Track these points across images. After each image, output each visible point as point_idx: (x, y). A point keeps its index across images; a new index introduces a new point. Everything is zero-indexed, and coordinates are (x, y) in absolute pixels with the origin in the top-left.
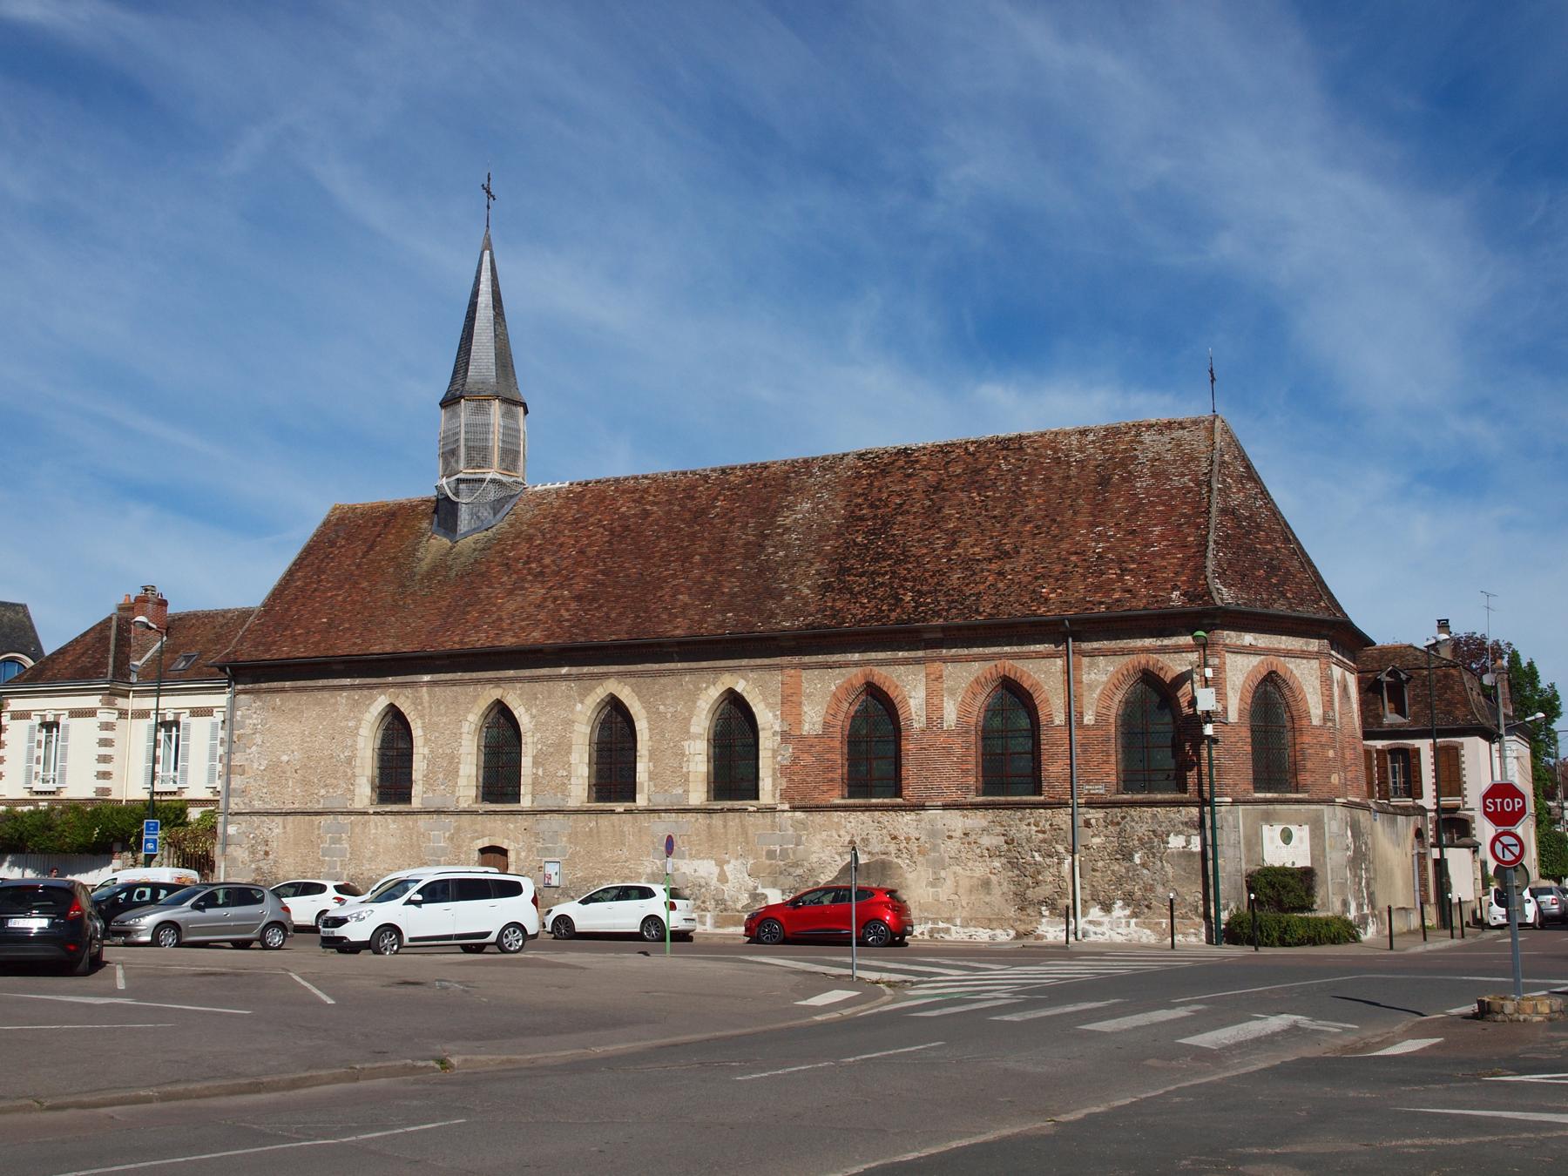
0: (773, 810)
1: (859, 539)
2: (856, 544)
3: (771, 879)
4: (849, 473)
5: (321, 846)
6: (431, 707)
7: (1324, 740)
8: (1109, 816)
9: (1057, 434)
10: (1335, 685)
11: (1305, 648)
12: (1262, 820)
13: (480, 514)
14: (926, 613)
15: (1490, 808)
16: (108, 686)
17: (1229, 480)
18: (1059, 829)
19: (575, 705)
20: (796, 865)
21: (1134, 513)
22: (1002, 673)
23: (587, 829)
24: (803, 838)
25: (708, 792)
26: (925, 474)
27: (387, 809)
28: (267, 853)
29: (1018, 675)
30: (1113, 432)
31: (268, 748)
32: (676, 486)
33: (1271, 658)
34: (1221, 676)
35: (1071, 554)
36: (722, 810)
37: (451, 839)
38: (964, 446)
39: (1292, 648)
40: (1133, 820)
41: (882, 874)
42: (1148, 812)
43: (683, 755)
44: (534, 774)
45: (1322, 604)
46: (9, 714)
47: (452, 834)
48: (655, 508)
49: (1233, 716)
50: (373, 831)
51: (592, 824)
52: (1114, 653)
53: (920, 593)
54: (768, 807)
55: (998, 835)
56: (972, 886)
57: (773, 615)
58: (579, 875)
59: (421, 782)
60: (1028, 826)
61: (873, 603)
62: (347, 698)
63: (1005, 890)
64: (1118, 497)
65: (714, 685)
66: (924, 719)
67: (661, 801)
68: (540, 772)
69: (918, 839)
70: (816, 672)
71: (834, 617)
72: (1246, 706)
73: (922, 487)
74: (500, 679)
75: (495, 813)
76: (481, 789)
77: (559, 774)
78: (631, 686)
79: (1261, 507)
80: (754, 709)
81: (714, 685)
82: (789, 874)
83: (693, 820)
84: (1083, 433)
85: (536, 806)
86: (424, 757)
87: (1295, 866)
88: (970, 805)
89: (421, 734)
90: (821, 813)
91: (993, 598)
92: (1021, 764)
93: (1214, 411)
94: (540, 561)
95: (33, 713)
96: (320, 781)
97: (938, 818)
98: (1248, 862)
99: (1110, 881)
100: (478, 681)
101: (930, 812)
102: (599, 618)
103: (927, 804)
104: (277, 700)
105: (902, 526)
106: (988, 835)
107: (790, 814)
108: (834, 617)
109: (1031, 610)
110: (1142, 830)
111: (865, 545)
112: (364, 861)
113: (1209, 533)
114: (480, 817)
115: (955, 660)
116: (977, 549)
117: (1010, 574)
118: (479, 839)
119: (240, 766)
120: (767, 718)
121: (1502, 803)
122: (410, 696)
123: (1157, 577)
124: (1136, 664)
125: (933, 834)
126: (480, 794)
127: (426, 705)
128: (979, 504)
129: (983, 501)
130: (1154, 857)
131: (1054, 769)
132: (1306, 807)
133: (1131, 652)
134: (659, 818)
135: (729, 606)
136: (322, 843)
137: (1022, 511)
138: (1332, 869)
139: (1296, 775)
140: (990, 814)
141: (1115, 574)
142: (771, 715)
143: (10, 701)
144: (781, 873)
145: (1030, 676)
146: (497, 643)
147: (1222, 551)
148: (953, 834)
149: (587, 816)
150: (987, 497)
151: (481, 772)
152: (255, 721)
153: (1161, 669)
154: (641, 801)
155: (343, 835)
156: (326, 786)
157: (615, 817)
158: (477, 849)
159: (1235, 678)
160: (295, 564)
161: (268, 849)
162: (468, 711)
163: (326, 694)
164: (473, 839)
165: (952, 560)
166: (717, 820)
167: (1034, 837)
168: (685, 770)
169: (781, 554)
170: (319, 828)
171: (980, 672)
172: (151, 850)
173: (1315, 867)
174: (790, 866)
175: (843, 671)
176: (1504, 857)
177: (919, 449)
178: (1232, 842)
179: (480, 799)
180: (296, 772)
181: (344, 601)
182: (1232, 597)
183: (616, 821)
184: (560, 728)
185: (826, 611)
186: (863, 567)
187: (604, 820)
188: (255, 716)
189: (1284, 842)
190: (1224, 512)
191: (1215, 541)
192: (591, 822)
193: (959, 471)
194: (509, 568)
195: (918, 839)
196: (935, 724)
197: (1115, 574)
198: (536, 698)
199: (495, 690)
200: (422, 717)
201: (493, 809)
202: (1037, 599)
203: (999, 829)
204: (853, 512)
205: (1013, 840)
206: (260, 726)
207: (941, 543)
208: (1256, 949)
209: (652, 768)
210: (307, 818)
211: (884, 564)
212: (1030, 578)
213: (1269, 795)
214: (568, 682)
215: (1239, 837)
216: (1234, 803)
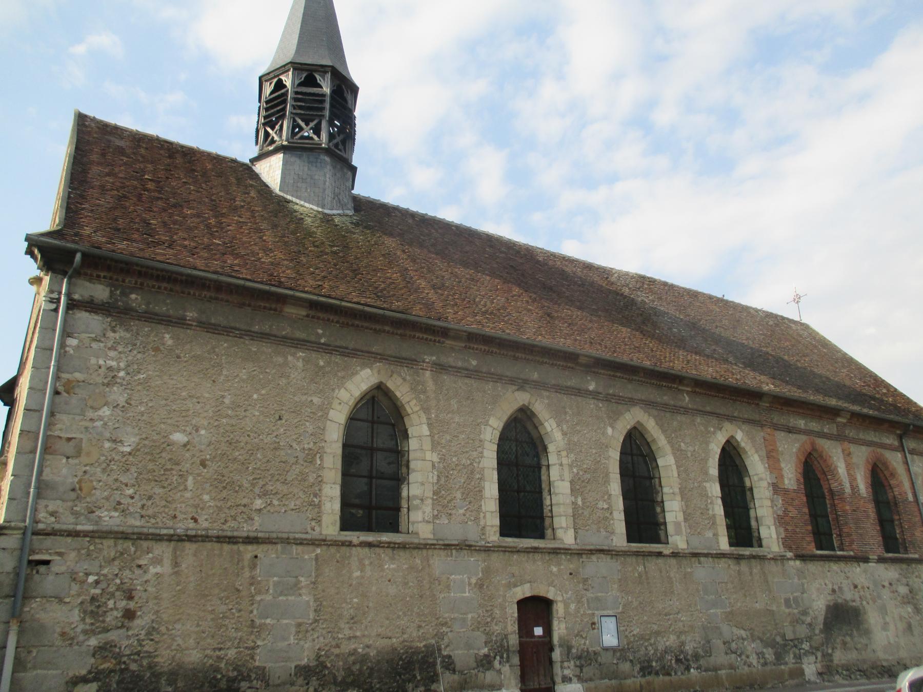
23: (637, 575)
28: (129, 615)
31: (142, 414)
37: (480, 586)
44: (573, 503)
47: (480, 579)
50: (358, 574)
51: (641, 568)
58: (635, 632)
59: (430, 501)
62: (306, 361)
68: (580, 502)
78: (655, 417)
82: (803, 623)
86: (433, 466)
89: (428, 433)
96: (253, 485)
100: (499, 378)
112: (342, 625)
118: (515, 586)
119: (69, 439)
122: (408, 378)
136: (259, 592)
152: (114, 364)
155: (302, 579)
157: (660, 561)
158: (516, 601)
161: (132, 605)
163: (267, 348)
164: (512, 585)
166: (744, 566)
168: (710, 512)
170: (253, 566)
184: (594, 451)
188: (112, 354)
195: (868, 588)
198: (566, 413)
199: (516, 393)
200: (426, 410)
203: (904, 581)
206: (122, 374)
209: (684, 507)
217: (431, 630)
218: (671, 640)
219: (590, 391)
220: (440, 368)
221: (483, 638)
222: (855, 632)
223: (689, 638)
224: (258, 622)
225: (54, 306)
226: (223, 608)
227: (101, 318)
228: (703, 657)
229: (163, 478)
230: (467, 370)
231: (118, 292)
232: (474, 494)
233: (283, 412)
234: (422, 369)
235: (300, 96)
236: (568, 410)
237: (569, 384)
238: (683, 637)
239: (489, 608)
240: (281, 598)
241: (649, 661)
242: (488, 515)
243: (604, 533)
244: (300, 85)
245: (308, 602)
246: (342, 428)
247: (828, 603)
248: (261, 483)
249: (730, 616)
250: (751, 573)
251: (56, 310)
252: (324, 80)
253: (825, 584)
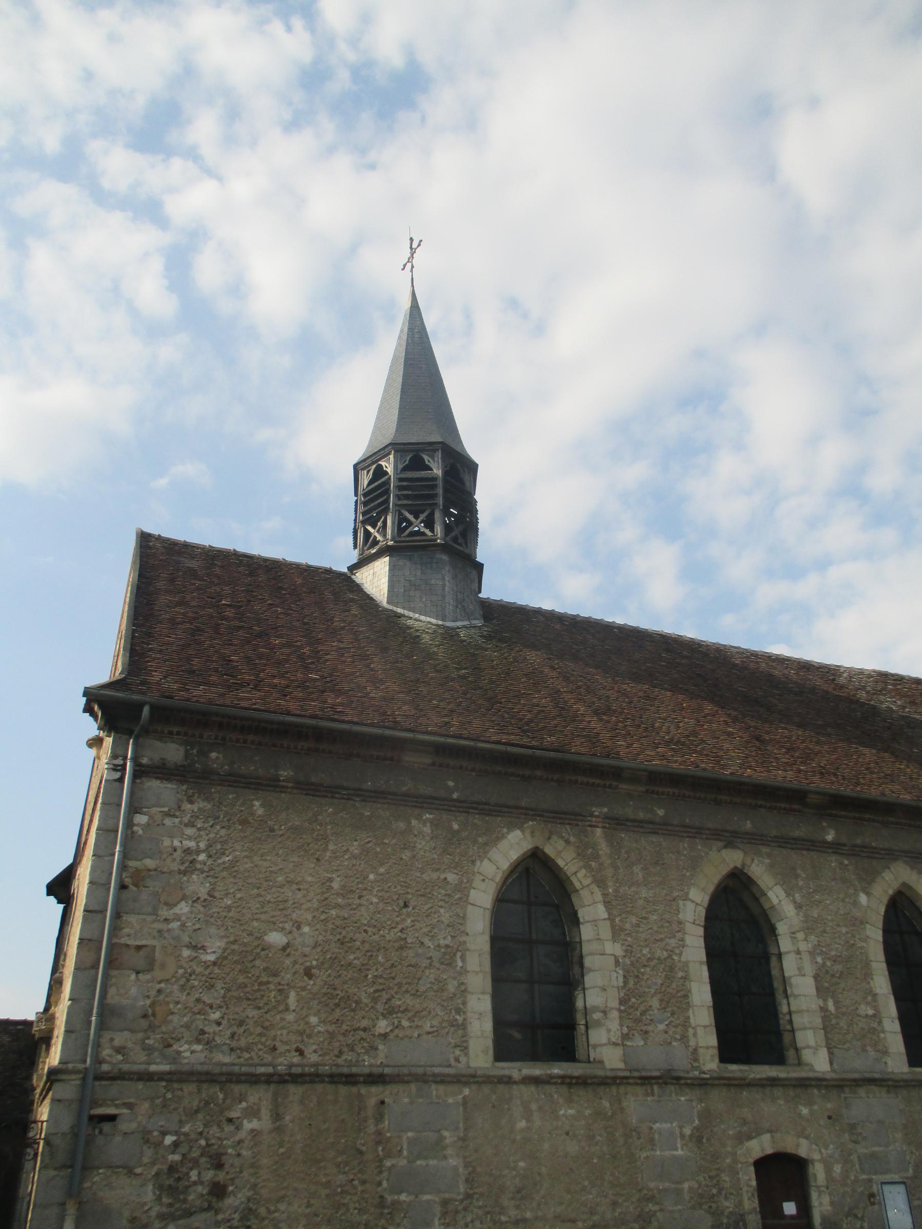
5: (388, 1163)
6: (616, 868)
28: (218, 1191)
31: (229, 908)
37: (697, 1138)
44: (821, 1008)
47: (697, 1129)
50: (522, 1124)
59: (615, 1014)
86: (617, 963)
89: (606, 916)
96: (375, 1000)
100: (696, 832)
112: (506, 1203)
118: (750, 1138)
119: (139, 948)
122: (572, 839)
136: (389, 1155)
152: (192, 844)
155: (446, 1133)
158: (752, 1161)
161: (221, 1176)
164: (742, 1138)
170: (379, 1117)
180: (308, 973)
184: (844, 930)
188: (189, 831)
199: (724, 852)
200: (600, 883)
206: (202, 857)
217: (631, 1209)
219: (829, 843)
220: (616, 823)
224: (389, 1198)
225: (117, 775)
226: (342, 1178)
227: (174, 786)
229: (258, 994)
230: (652, 823)
231: (195, 751)
233: (410, 896)
234: (591, 826)
235: (405, 483)
236: (799, 872)
237: (796, 833)
239: (713, 1173)
240: (419, 1162)
242: (700, 1031)
243: (872, 1054)
244: (404, 469)
245: (456, 1168)
246: (488, 914)
248: (385, 996)
251: (121, 780)
252: (434, 460)
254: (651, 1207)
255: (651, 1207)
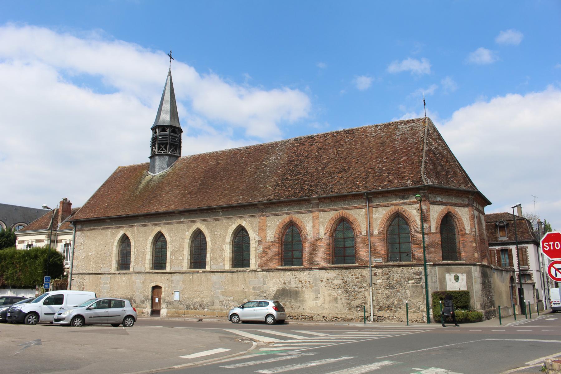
0: (255, 271)
1: (291, 168)
2: (290, 170)
3: (254, 298)
4: (290, 146)
5: (101, 285)
6: (137, 235)
7: (471, 239)
8: (384, 271)
9: (366, 127)
10: (476, 218)
11: (462, 203)
12: (446, 272)
13: (163, 167)
14: (312, 193)
15: (546, 245)
16: (47, 231)
17: (431, 139)
18: (364, 277)
19: (186, 232)
20: (264, 292)
21: (394, 153)
22: (341, 215)
23: (189, 279)
24: (266, 282)
25: (232, 264)
26: (317, 144)
27: (122, 272)
29: (348, 216)
30: (388, 126)
31: (85, 250)
32: (230, 154)
33: (449, 207)
34: (428, 213)
35: (369, 169)
36: (237, 271)
37: (143, 283)
38: (332, 134)
39: (457, 202)
40: (393, 273)
41: (296, 296)
42: (399, 270)
43: (223, 250)
45: (469, 185)
46: (18, 242)
47: (143, 281)
48: (222, 162)
49: (433, 229)
50: (118, 280)
51: (191, 277)
52: (385, 206)
53: (311, 186)
54: (253, 270)
55: (341, 280)
56: (330, 300)
57: (256, 196)
58: (186, 297)
59: (133, 262)
60: (351, 276)
61: (293, 190)
62: (111, 232)
63: (343, 302)
64: (388, 148)
65: (234, 223)
66: (312, 234)
67: (215, 268)
68: (173, 258)
69: (309, 282)
70: (272, 217)
71: (278, 196)
72: (438, 225)
73: (316, 148)
74: (160, 224)
75: (158, 273)
76: (154, 264)
77: (180, 259)
78: (205, 225)
79: (444, 149)
80: (248, 232)
81: (234, 223)
82: (261, 296)
83: (226, 275)
84: (376, 126)
85: (172, 270)
86: (135, 253)
87: (461, 290)
88: (329, 268)
90: (273, 272)
91: (338, 186)
92: (350, 251)
93: (426, 116)
94: (179, 181)
95: (25, 241)
97: (317, 273)
98: (440, 289)
99: (384, 297)
100: (153, 225)
101: (314, 271)
102: (195, 200)
103: (313, 268)
104: (88, 233)
105: (307, 163)
106: (336, 280)
107: (261, 273)
108: (278, 196)
109: (352, 190)
110: (397, 277)
111: (293, 170)
112: (114, 291)
113: (422, 158)
114: (153, 275)
115: (323, 211)
116: (334, 169)
117: (345, 177)
118: (152, 283)
120: (253, 236)
121: (553, 245)
123: (402, 175)
124: (394, 210)
125: (315, 280)
126: (153, 266)
127: (136, 234)
128: (336, 153)
129: (338, 152)
130: (402, 288)
131: (362, 253)
132: (464, 266)
133: (392, 205)
134: (214, 275)
135: (241, 194)
137: (352, 155)
138: (476, 291)
139: (460, 253)
140: (337, 271)
141: (386, 175)
142: (255, 234)
143: (19, 237)
144: (258, 296)
145: (352, 216)
146: (159, 210)
147: (428, 165)
148: (323, 279)
149: (189, 274)
150: (339, 150)
151: (154, 258)
152: (81, 241)
153: (404, 211)
154: (208, 268)
156: (103, 264)
157: (199, 274)
159: (434, 214)
160: (101, 186)
161: (84, 287)
162: (149, 235)
165: (324, 173)
166: (235, 275)
167: (354, 280)
168: (223, 256)
169: (262, 175)
171: (333, 215)
172: (47, 287)
173: (469, 290)
174: (261, 293)
175: (282, 216)
176: (556, 276)
177: (316, 136)
178: (433, 281)
179: (153, 268)
180: (94, 259)
181: (114, 198)
182: (431, 182)
183: (199, 277)
184: (180, 241)
185: (275, 194)
186: (291, 177)
187: (195, 276)
188: (81, 239)
189: (455, 280)
190: (428, 151)
191: (425, 162)
192: (190, 276)
193: (330, 142)
194: (169, 185)
195: (309, 282)
196: (316, 236)
197: (386, 175)
199: (158, 227)
200: (134, 238)
201: (157, 272)
202: (355, 186)
203: (341, 278)
204: (290, 159)
205: (346, 282)
206: (83, 243)
207: (320, 168)
208: (444, 326)
209: (212, 255)
210: (96, 275)
211: (299, 176)
212: (353, 179)
213: (449, 262)
214: (183, 224)
215: (437, 278)
216: (434, 265)
218: (199, 300)
220: (138, 226)
221: (143, 296)
222: (293, 300)
223: (205, 299)
224: (101, 290)
228: (210, 305)
232: (144, 259)
236: (173, 229)
238: (203, 299)
241: (190, 305)
243: (180, 267)
247: (278, 288)
249: (225, 293)
250: (238, 278)
253: (280, 281)
254: (134, 293)
255: (134, 293)
